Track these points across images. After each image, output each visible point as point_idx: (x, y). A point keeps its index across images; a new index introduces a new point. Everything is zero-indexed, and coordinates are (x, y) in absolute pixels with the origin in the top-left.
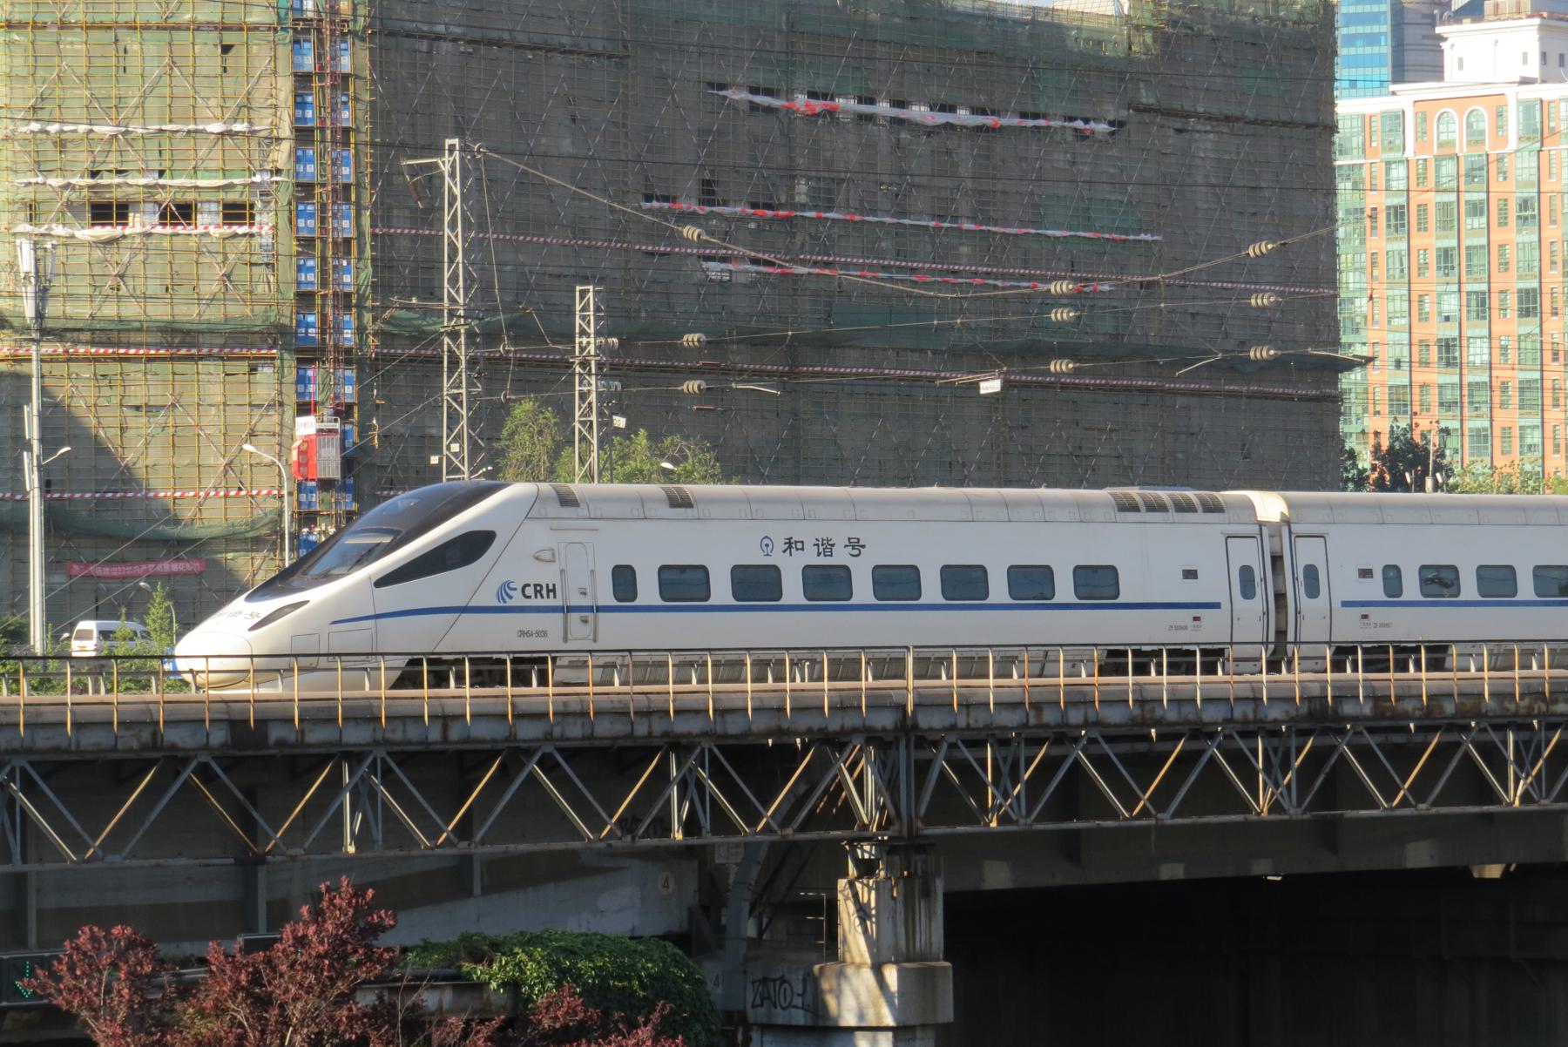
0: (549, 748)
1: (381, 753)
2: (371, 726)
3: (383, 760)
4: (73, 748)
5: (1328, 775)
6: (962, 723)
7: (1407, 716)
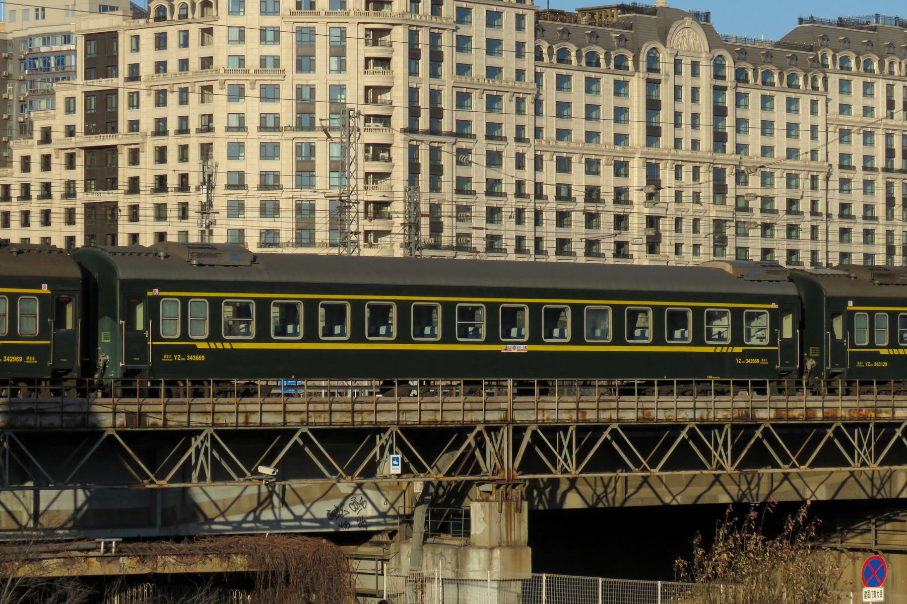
0: (305, 429)
1: (210, 431)
2: (205, 416)
3: (212, 435)
4: (38, 425)
5: (749, 450)
6: (540, 417)
7: (794, 418)
